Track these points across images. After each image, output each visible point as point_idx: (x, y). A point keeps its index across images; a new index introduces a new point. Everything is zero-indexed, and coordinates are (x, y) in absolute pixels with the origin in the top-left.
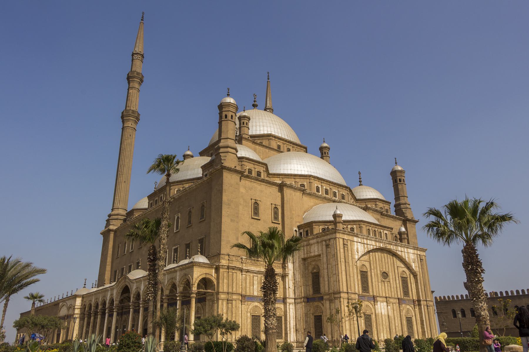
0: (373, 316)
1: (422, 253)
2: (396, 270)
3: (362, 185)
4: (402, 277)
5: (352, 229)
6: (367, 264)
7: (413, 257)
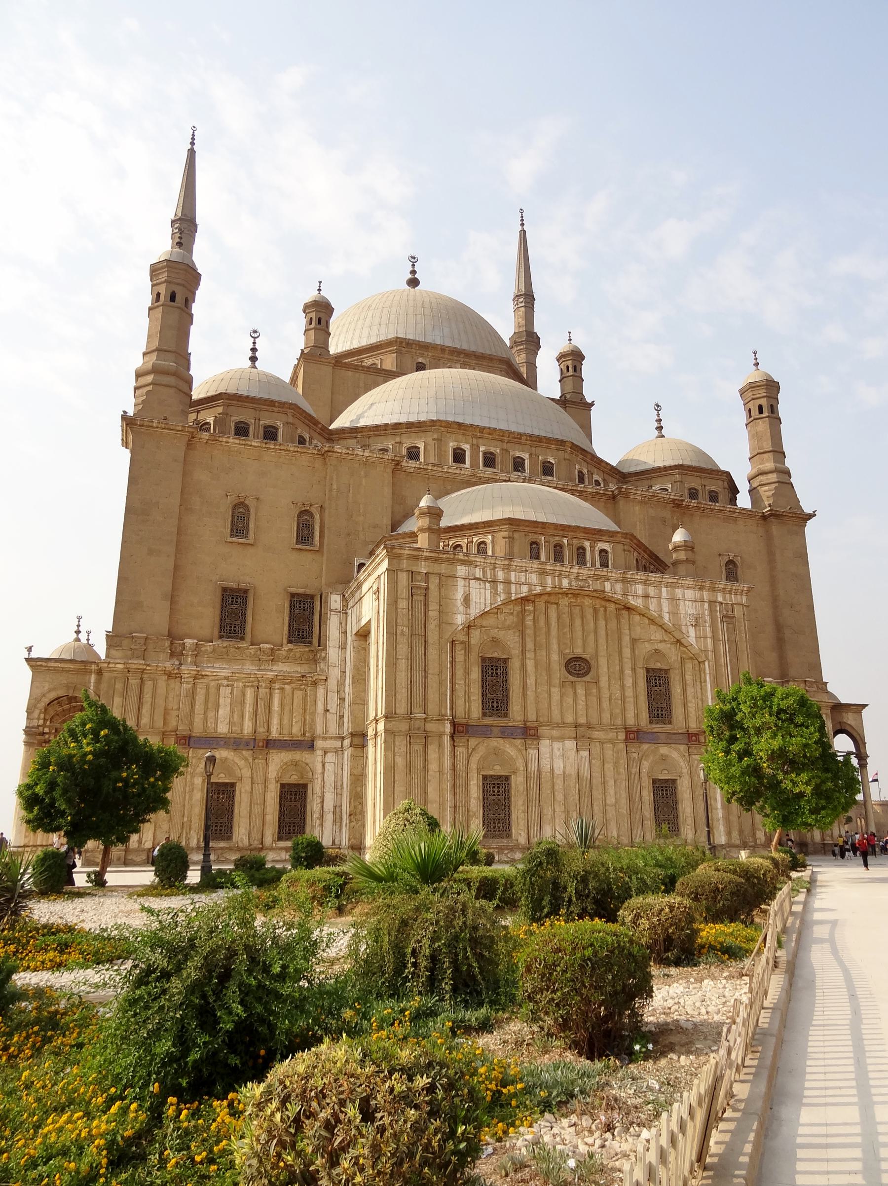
0: (517, 782)
1: (734, 599)
2: (627, 652)
3: (663, 436)
4: (648, 670)
5: (482, 548)
6: (511, 640)
7: (691, 611)
